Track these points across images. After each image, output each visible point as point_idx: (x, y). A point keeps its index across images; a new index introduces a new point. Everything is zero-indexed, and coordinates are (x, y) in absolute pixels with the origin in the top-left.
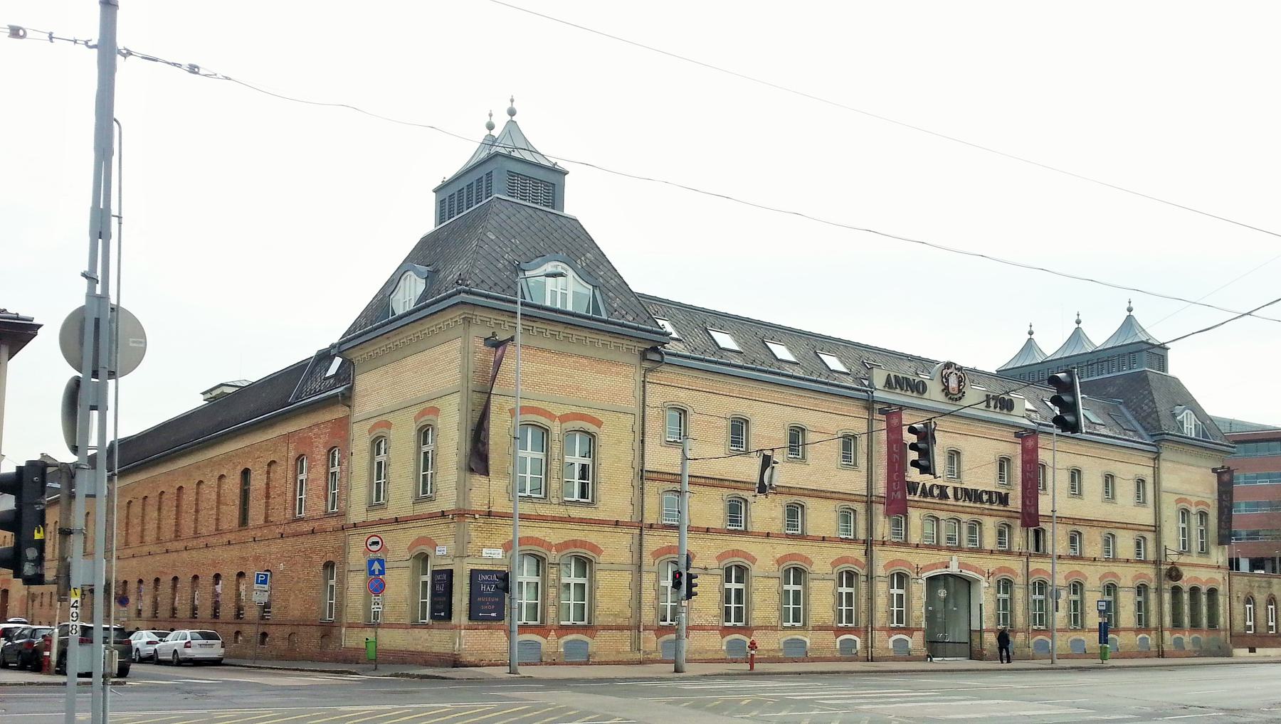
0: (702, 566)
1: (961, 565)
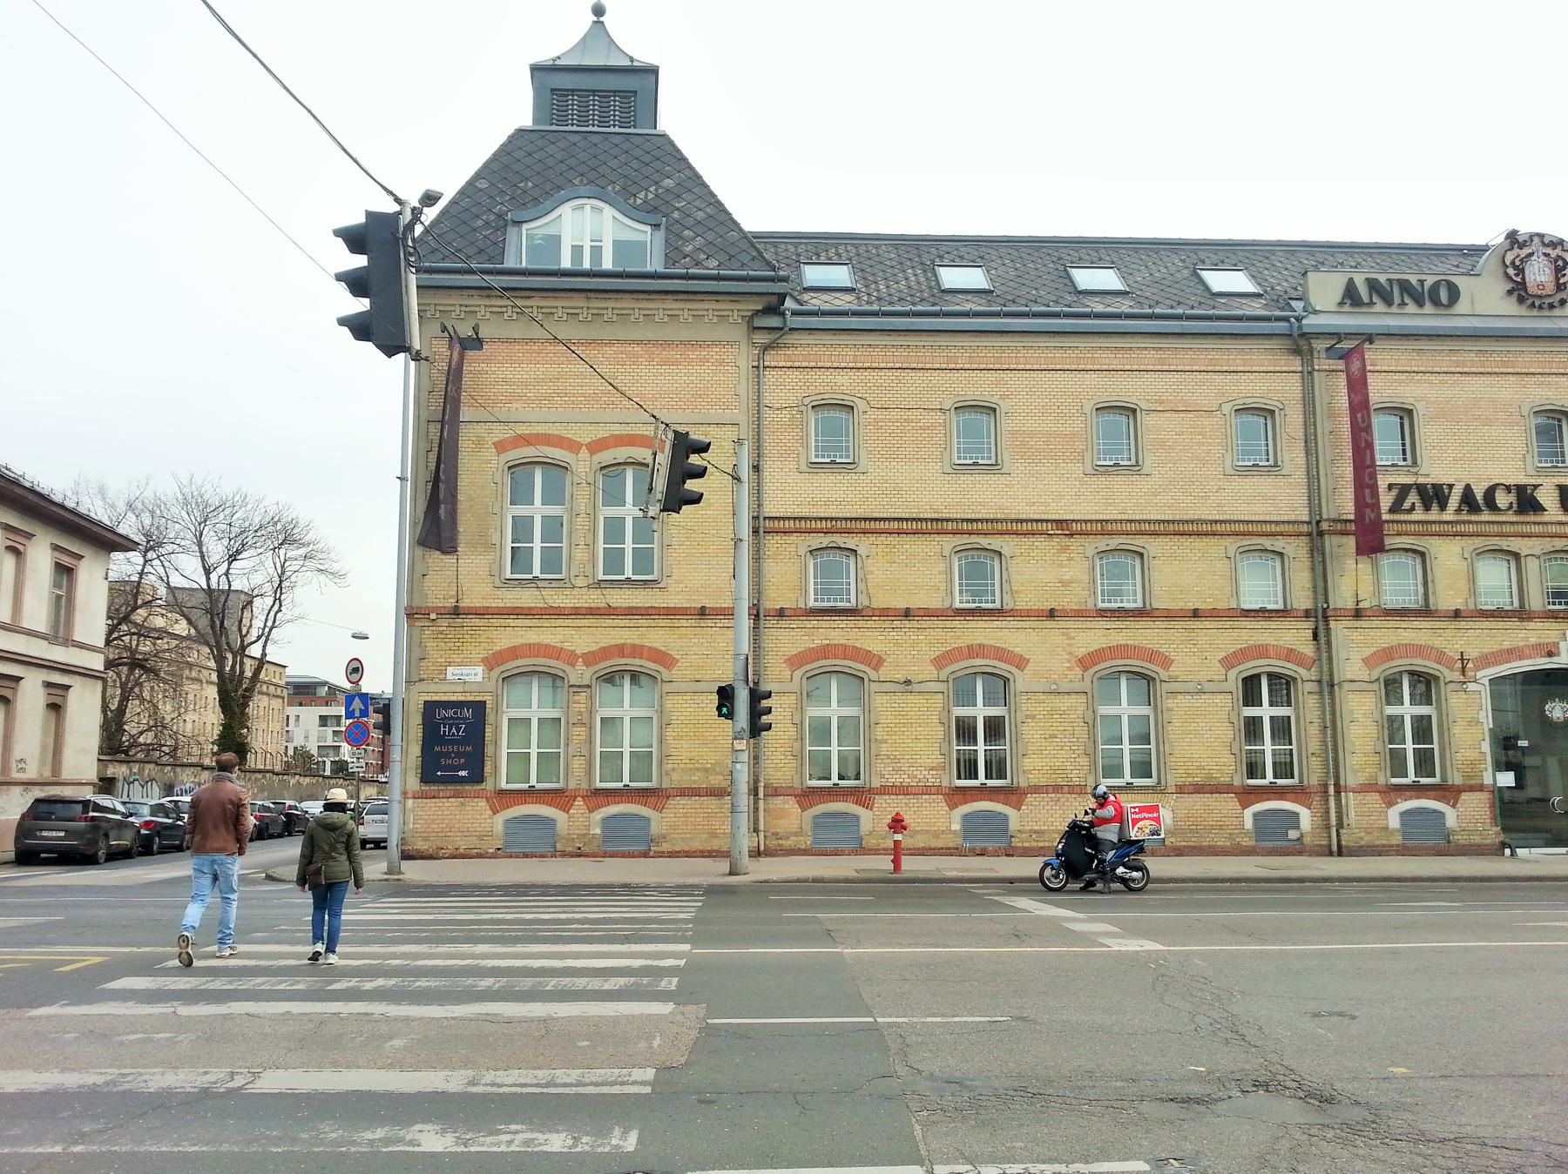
0: (901, 677)
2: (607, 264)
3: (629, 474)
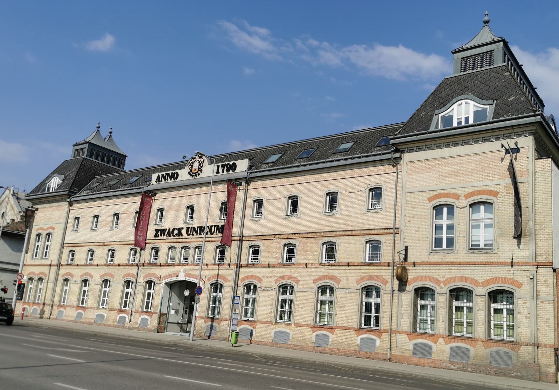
1: (187, 275)
2: (471, 122)
3: (445, 210)
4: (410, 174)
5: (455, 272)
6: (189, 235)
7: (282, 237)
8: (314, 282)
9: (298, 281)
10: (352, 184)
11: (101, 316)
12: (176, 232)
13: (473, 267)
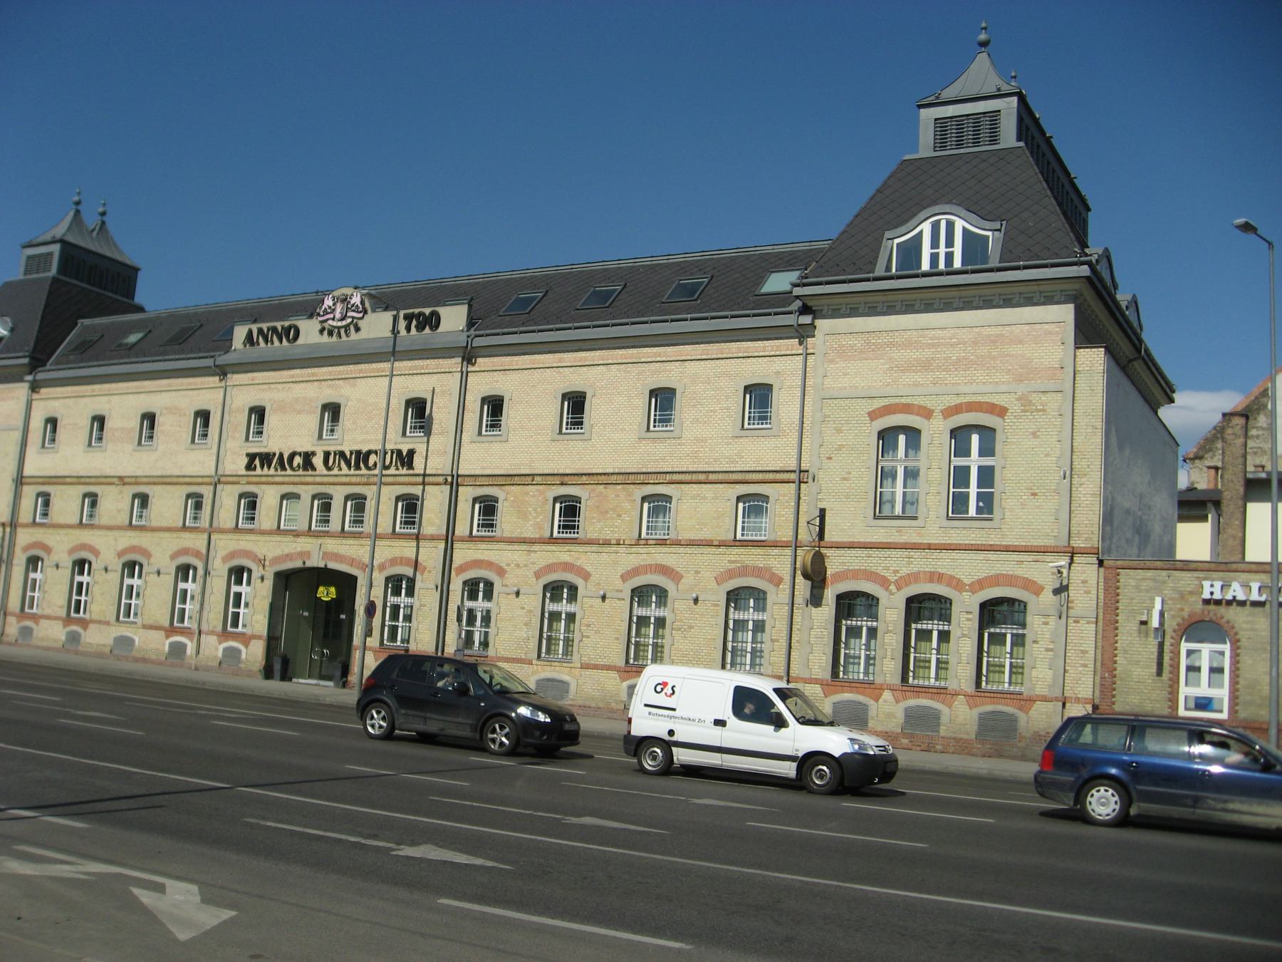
4: (832, 361)
5: (920, 562)
6: (329, 469)
7: (550, 480)
8: (624, 577)
9: (586, 576)
10: (709, 376)
11: (125, 642)
12: (298, 460)
13: (954, 554)
